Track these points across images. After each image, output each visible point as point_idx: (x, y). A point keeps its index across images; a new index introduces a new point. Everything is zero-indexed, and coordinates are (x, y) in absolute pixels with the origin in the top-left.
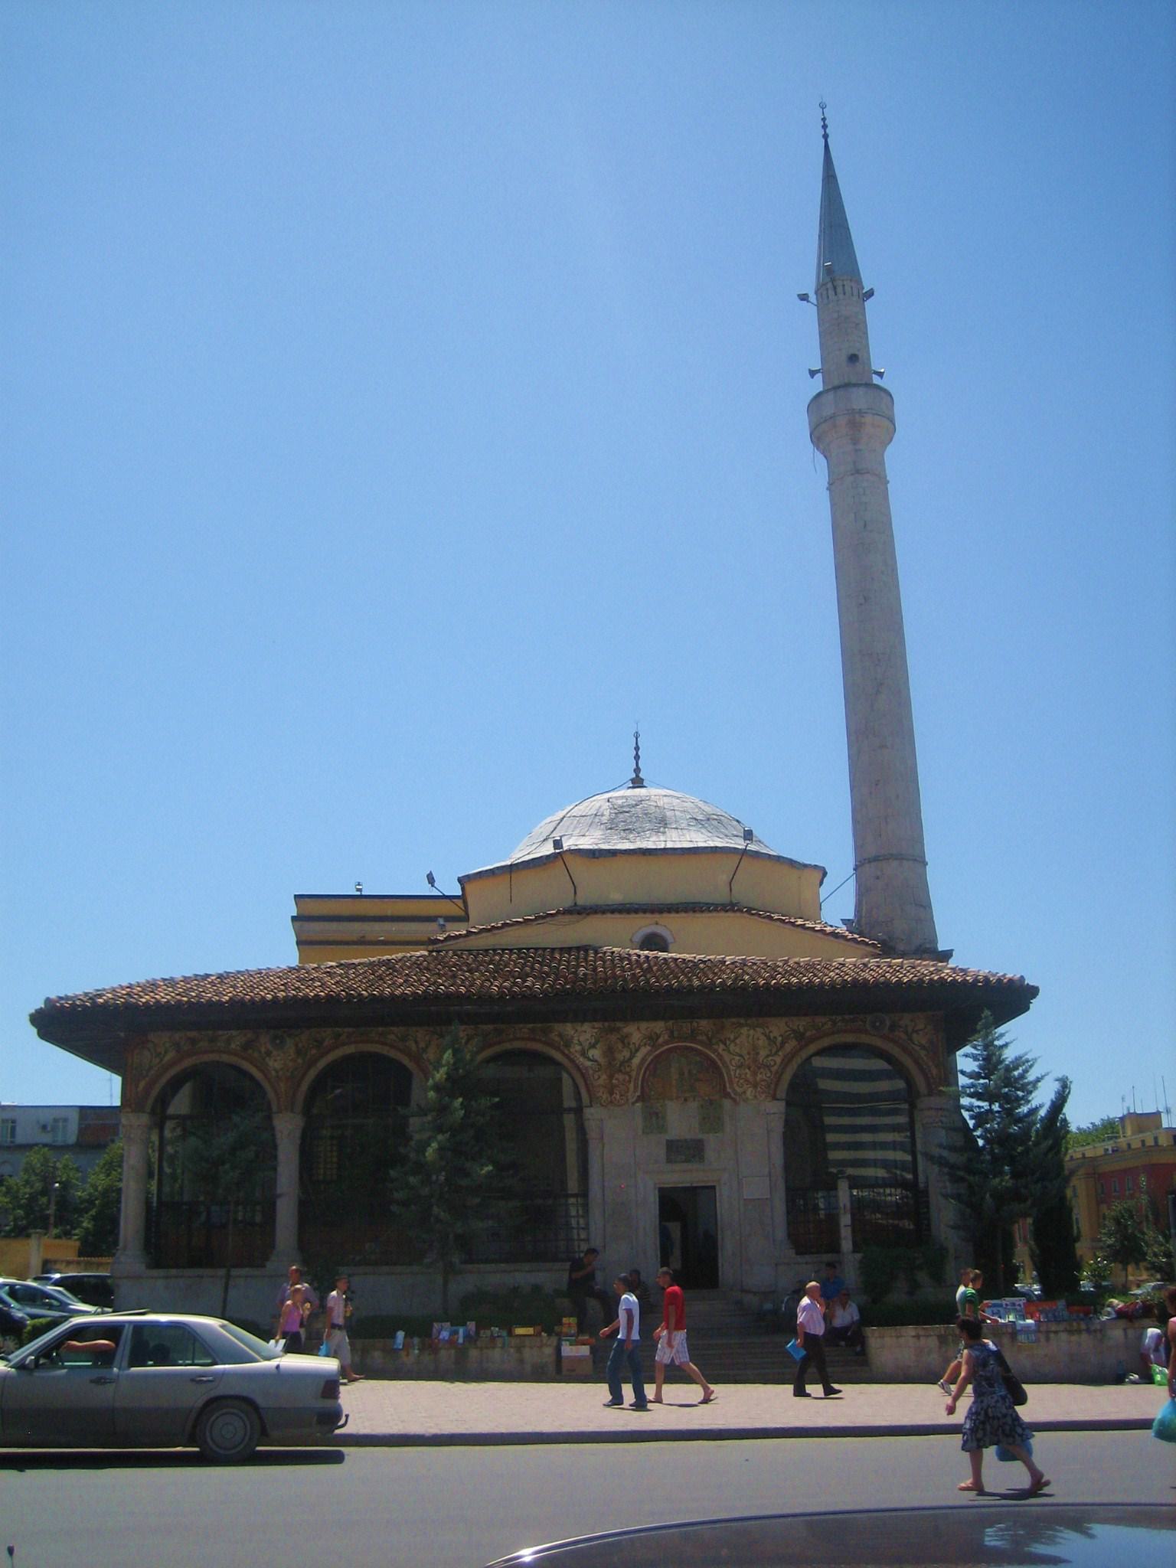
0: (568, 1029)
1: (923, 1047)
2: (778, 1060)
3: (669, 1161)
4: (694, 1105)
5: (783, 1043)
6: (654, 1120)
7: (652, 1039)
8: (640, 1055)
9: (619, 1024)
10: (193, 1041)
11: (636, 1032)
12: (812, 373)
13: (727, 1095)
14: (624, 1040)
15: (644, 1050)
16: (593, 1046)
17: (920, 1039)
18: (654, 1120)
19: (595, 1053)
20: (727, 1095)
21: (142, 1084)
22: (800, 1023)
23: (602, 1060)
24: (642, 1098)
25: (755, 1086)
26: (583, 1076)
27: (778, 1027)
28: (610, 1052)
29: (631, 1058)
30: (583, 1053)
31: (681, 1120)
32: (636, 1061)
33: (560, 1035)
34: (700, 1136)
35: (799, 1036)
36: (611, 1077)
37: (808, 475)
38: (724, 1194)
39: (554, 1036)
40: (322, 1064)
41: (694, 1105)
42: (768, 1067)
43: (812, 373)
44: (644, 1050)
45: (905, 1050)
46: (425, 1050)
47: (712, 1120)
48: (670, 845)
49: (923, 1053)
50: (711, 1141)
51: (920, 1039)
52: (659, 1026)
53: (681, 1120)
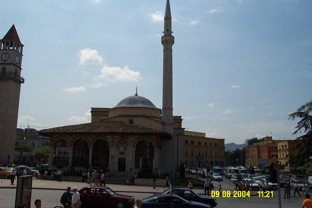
0: (107, 136)
1: (155, 141)
2: (135, 141)
3: (120, 154)
4: (123, 147)
5: (136, 139)
6: (118, 149)
7: (118, 138)
8: (116, 140)
9: (114, 136)
10: (59, 136)
11: (116, 137)
12: (163, 32)
13: (128, 146)
14: (115, 138)
15: (117, 139)
16: (110, 139)
17: (154, 139)
18: (118, 149)
19: (111, 140)
20: (128, 146)
21: (53, 142)
22: (138, 137)
23: (112, 141)
24: (117, 146)
25: (132, 145)
26: (109, 143)
27: (135, 137)
28: (113, 140)
29: (116, 140)
30: (109, 140)
31: (122, 149)
32: (116, 141)
33: (106, 137)
34: (124, 151)
35: (138, 138)
36: (113, 143)
37: (161, 48)
38: (127, 159)
39: (105, 137)
40: (76, 140)
41: (123, 147)
42: (133, 142)
43: (163, 32)
44: (117, 139)
45: (152, 141)
46: (89, 138)
47: (126, 149)
48: (135, 106)
49: (154, 141)
50: (125, 152)
51: (154, 139)
52: (119, 136)
53: (122, 149)
